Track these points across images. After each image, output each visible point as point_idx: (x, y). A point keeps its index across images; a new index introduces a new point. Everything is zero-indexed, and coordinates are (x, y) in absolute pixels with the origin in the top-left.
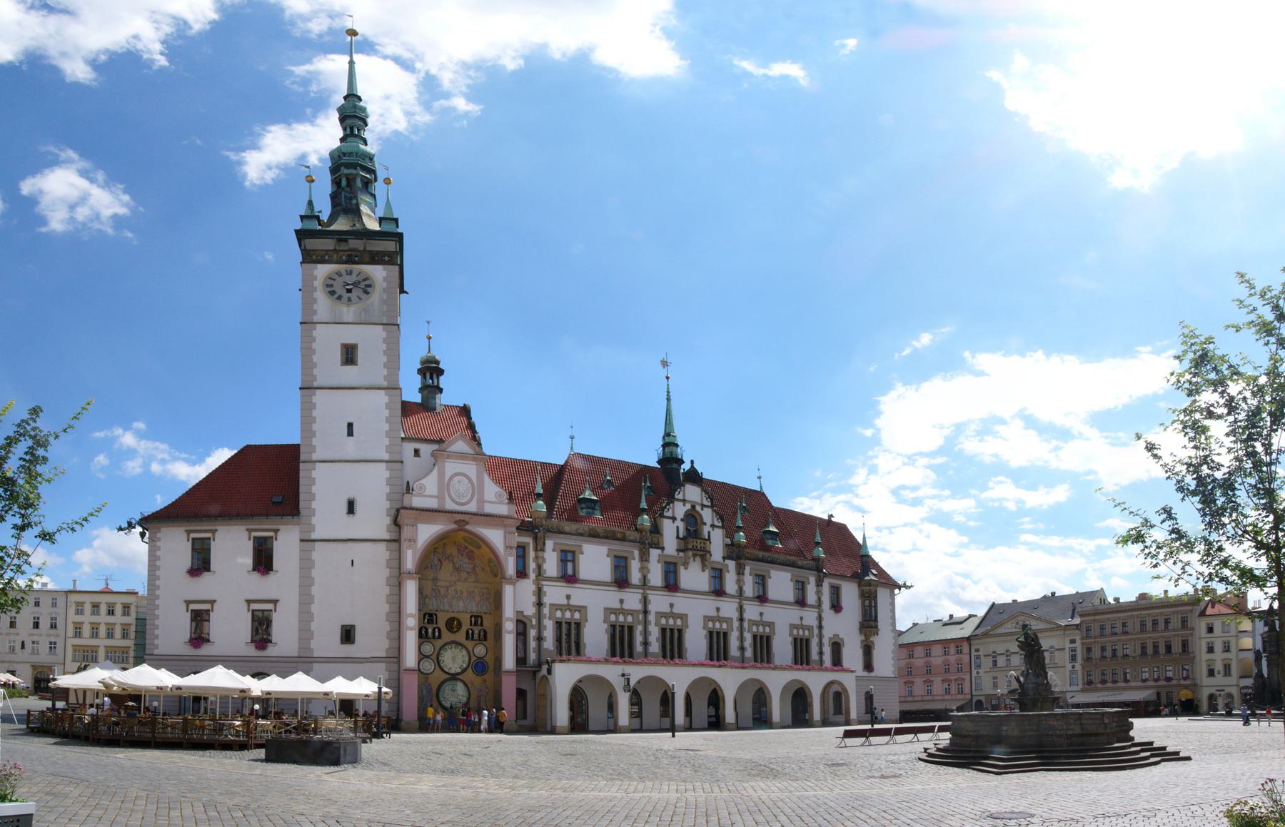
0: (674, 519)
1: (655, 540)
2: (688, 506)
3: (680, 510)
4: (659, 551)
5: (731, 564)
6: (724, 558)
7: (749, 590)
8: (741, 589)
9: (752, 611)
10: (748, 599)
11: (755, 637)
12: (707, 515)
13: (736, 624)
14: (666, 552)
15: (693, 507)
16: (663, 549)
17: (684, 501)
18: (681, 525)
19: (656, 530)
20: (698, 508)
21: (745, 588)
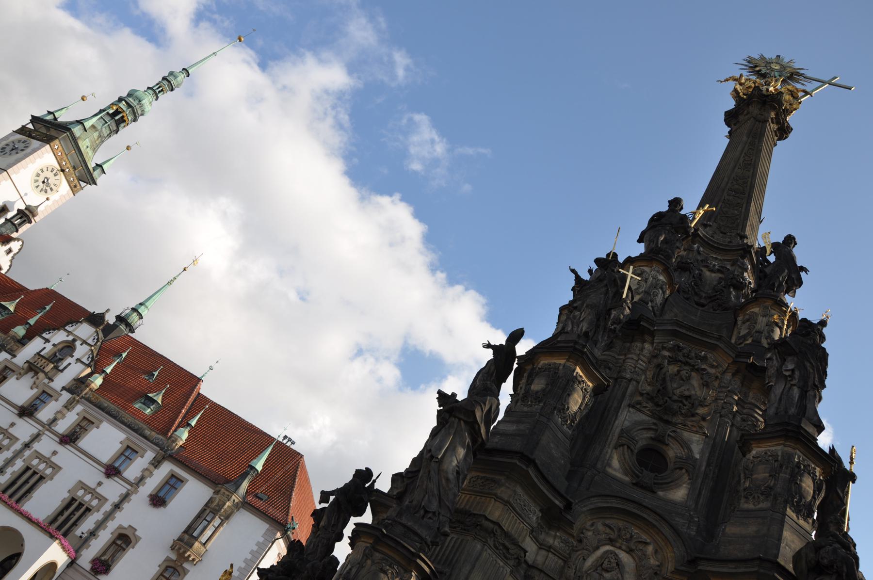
0: (47, 341)
1: (15, 347)
2: (70, 338)
3: (59, 337)
4: (8, 356)
5: (66, 396)
6: (64, 388)
7: (63, 426)
8: (55, 420)
9: (46, 445)
10: (55, 433)
11: (28, 468)
12: (81, 351)
13: (18, 446)
14: (15, 360)
15: (74, 340)
16: (14, 356)
17: (69, 333)
18: (49, 347)
19: (23, 342)
20: (78, 343)
21: (60, 422)
